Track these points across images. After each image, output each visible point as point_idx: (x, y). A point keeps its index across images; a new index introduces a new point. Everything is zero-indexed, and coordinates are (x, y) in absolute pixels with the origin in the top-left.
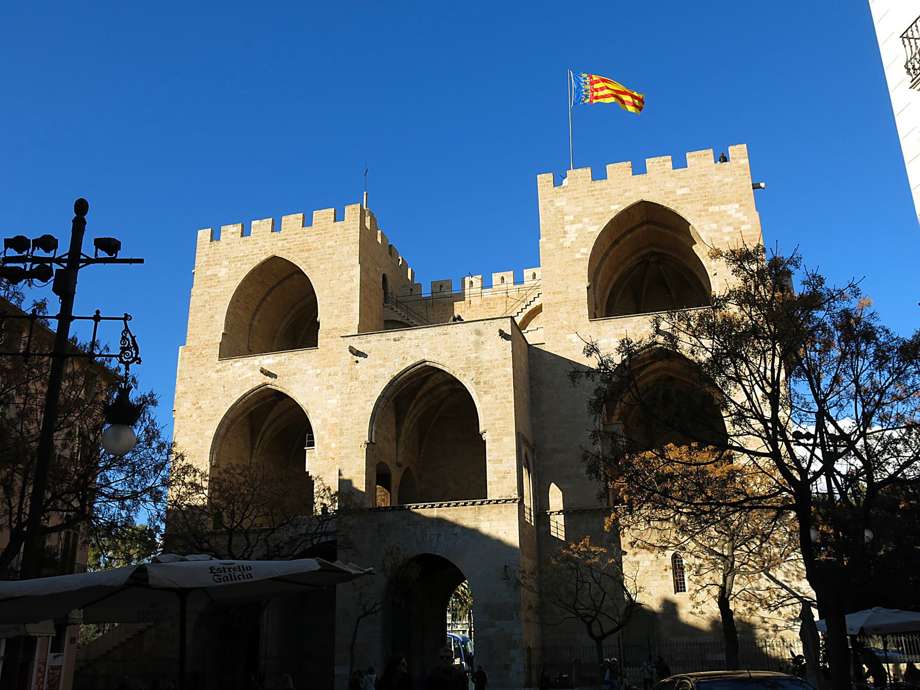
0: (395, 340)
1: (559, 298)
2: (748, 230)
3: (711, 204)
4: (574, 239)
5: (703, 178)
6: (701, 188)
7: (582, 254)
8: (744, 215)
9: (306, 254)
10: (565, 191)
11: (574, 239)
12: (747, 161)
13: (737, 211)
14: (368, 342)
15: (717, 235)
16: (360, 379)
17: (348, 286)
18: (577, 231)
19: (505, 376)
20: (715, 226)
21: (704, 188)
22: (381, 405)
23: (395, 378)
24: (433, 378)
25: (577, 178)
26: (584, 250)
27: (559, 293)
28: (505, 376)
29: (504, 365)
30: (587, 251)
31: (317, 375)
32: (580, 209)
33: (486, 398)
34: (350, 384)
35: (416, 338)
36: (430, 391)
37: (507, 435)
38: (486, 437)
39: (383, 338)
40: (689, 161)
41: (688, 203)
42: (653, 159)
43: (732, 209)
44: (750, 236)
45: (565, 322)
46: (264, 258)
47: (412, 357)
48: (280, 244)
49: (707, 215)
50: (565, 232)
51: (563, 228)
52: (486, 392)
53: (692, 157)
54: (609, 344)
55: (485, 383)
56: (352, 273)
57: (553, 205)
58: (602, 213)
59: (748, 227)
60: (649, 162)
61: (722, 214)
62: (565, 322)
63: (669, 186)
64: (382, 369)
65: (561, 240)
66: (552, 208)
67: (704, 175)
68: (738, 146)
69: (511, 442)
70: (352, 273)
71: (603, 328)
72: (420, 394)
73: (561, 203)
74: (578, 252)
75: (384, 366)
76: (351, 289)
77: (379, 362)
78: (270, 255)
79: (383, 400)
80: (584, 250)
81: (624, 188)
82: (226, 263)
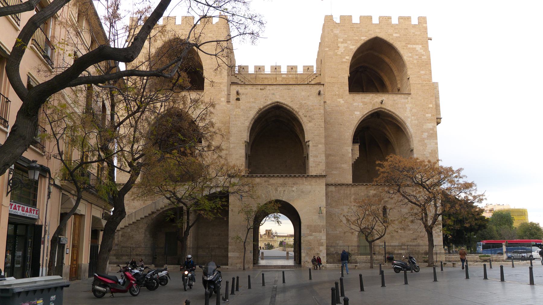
0: (261, 89)
3: (409, 44)
7: (347, 59)
13: (421, 49)
15: (411, 59)
18: (344, 47)
19: (320, 114)
20: (410, 55)
21: (406, 35)
23: (261, 109)
26: (347, 57)
27: (334, 77)
28: (320, 114)
29: (319, 109)
30: (348, 58)
32: (346, 36)
33: (310, 125)
37: (321, 144)
38: (310, 144)
39: (254, 88)
47: (271, 99)
50: (338, 47)
51: (337, 45)
52: (310, 121)
55: (309, 117)
63: (390, 31)
64: (254, 104)
65: (336, 51)
69: (321, 147)
74: (344, 58)
75: (255, 102)
77: (251, 100)
80: (347, 57)
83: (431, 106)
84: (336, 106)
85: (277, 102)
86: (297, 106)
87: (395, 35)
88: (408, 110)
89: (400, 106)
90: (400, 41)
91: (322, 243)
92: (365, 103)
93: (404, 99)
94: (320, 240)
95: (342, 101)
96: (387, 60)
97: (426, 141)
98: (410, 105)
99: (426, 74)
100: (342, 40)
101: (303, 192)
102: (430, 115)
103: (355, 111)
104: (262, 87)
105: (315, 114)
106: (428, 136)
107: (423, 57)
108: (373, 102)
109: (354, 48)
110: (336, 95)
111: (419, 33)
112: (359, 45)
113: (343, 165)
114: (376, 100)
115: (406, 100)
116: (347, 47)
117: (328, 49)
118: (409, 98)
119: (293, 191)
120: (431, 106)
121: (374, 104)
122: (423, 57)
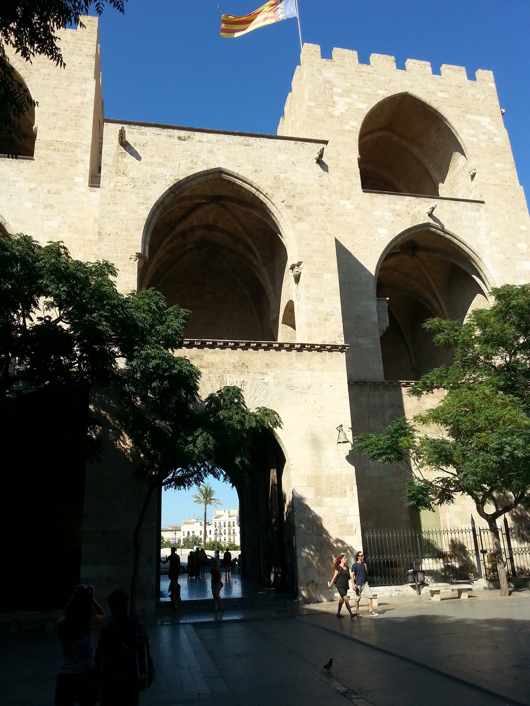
0: (180, 138)
3: (467, 112)
4: (343, 111)
6: (459, 97)
7: (352, 127)
10: (333, 65)
11: (343, 111)
12: (493, 85)
14: (142, 134)
15: (475, 140)
16: (131, 174)
17: (78, 100)
20: (472, 132)
22: (157, 213)
25: (344, 56)
30: (355, 125)
31: (31, 190)
33: (301, 226)
34: (116, 179)
35: (208, 142)
36: (184, 233)
41: (448, 106)
42: (414, 61)
43: (485, 121)
45: (338, 188)
47: (204, 162)
52: (299, 219)
55: (299, 208)
56: (84, 86)
57: (320, 74)
58: (370, 94)
60: (410, 63)
62: (338, 188)
64: (159, 170)
65: (330, 109)
66: (320, 77)
67: (460, 87)
68: (486, 71)
70: (84, 86)
72: (179, 228)
74: (348, 124)
75: (164, 166)
76: (82, 103)
77: (156, 159)
79: (161, 208)
81: (385, 78)
85: (219, 172)
86: (269, 183)
87: (440, 95)
90: (452, 107)
91: (351, 526)
94: (345, 517)
95: (349, 206)
96: (416, 151)
99: (504, 170)
100: (340, 91)
101: (290, 387)
104: (183, 133)
105: (312, 204)
107: (496, 139)
108: (412, 212)
109: (366, 107)
110: (335, 192)
112: (374, 103)
113: (361, 340)
114: (419, 208)
115: (477, 214)
117: (313, 104)
119: (267, 384)
121: (415, 216)
122: (496, 139)
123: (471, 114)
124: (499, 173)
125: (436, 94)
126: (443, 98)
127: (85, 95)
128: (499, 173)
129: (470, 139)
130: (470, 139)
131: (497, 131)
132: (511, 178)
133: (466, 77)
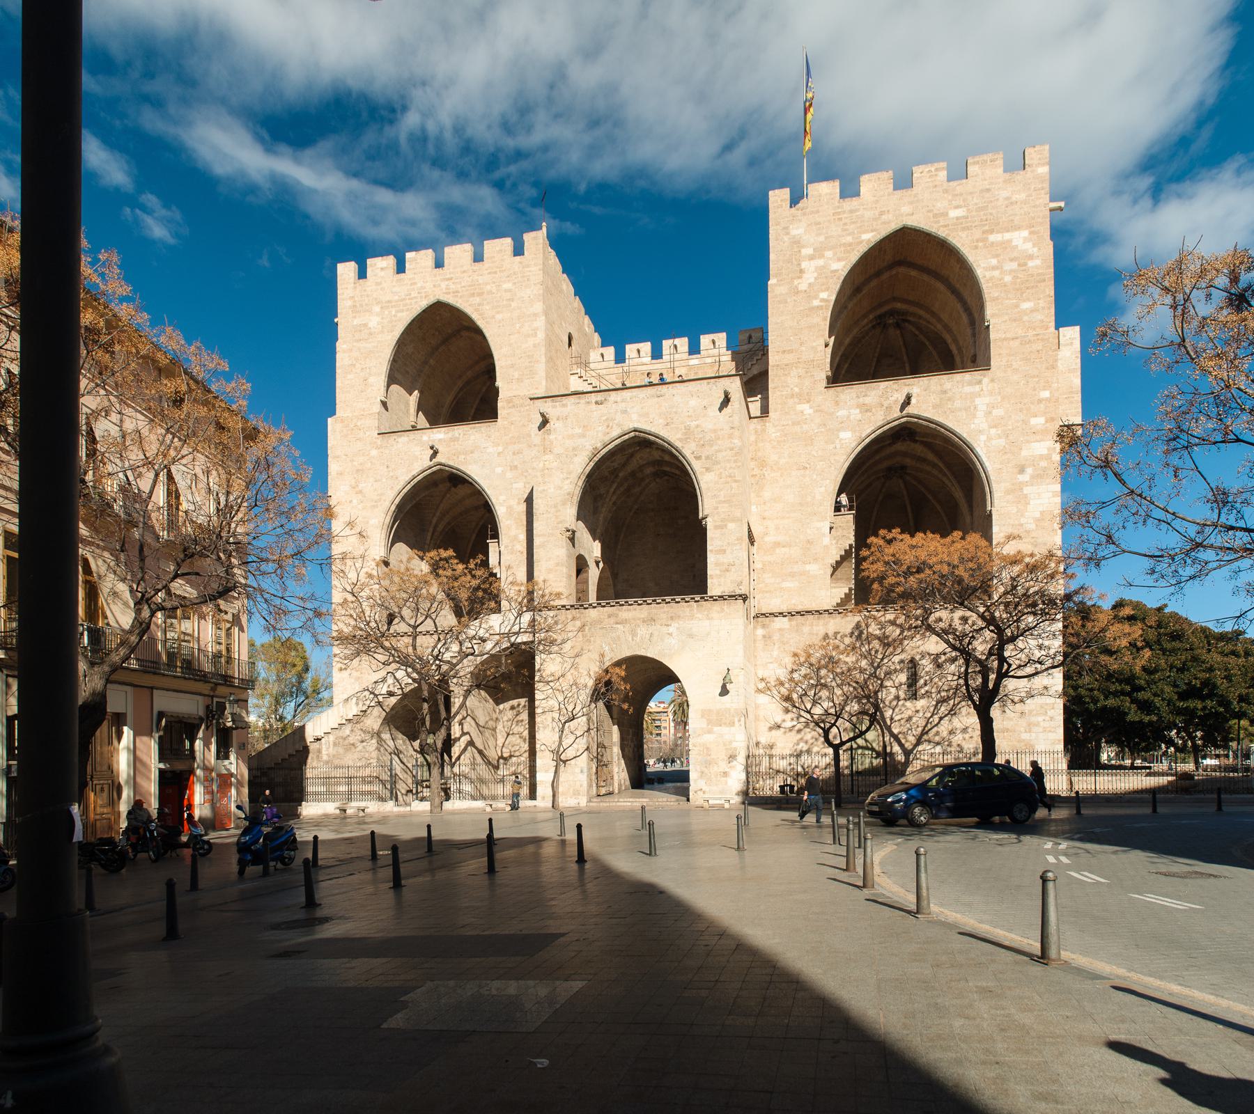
1: (789, 358)
2: (1037, 267)
3: (992, 232)
4: (812, 280)
5: (987, 195)
8: (1034, 246)
9: (477, 300)
10: (804, 214)
11: (812, 280)
13: (1025, 240)
15: (996, 273)
18: (816, 268)
20: (994, 262)
24: (638, 456)
27: (791, 351)
30: (828, 296)
40: (972, 169)
41: (963, 229)
43: (1019, 239)
44: (1039, 275)
45: (796, 390)
46: (424, 304)
48: (443, 285)
49: (985, 247)
50: (802, 271)
53: (974, 163)
54: (848, 417)
58: (850, 245)
59: (1038, 262)
61: (1006, 245)
63: (940, 205)
65: (796, 282)
66: (786, 238)
67: (988, 190)
71: (842, 397)
73: (797, 230)
74: (816, 297)
76: (535, 346)
78: (431, 300)
80: (824, 295)
82: (377, 309)
83: (1045, 394)
84: (793, 424)
88: (980, 414)
89: (958, 404)
90: (968, 228)
92: (866, 409)
93: (970, 384)
97: (1027, 490)
98: (987, 400)
102: (1041, 420)
103: (838, 430)
106: (1032, 477)
107: (1030, 264)
108: (886, 404)
109: (841, 266)
110: (792, 396)
111: (1023, 196)
112: (854, 257)
115: (977, 388)
116: (824, 267)
118: (986, 380)
120: (1045, 394)
121: (889, 408)
122: (1030, 264)
123: (998, 232)
124: (1025, 318)
125: (945, 214)
126: (958, 218)
127: (536, 335)
128: (1025, 318)
129: (988, 274)
130: (988, 274)
131: (1035, 249)
132: (1042, 321)
133: (1000, 170)
